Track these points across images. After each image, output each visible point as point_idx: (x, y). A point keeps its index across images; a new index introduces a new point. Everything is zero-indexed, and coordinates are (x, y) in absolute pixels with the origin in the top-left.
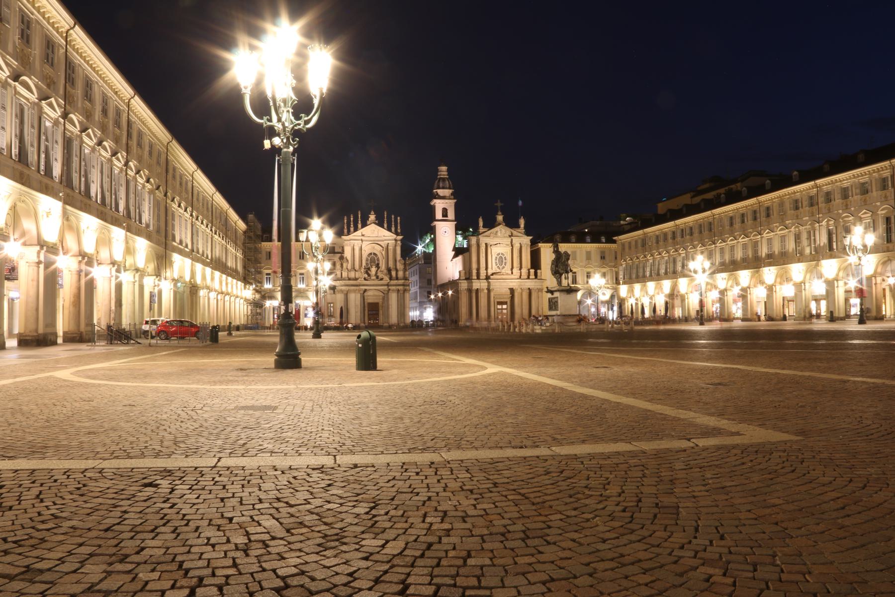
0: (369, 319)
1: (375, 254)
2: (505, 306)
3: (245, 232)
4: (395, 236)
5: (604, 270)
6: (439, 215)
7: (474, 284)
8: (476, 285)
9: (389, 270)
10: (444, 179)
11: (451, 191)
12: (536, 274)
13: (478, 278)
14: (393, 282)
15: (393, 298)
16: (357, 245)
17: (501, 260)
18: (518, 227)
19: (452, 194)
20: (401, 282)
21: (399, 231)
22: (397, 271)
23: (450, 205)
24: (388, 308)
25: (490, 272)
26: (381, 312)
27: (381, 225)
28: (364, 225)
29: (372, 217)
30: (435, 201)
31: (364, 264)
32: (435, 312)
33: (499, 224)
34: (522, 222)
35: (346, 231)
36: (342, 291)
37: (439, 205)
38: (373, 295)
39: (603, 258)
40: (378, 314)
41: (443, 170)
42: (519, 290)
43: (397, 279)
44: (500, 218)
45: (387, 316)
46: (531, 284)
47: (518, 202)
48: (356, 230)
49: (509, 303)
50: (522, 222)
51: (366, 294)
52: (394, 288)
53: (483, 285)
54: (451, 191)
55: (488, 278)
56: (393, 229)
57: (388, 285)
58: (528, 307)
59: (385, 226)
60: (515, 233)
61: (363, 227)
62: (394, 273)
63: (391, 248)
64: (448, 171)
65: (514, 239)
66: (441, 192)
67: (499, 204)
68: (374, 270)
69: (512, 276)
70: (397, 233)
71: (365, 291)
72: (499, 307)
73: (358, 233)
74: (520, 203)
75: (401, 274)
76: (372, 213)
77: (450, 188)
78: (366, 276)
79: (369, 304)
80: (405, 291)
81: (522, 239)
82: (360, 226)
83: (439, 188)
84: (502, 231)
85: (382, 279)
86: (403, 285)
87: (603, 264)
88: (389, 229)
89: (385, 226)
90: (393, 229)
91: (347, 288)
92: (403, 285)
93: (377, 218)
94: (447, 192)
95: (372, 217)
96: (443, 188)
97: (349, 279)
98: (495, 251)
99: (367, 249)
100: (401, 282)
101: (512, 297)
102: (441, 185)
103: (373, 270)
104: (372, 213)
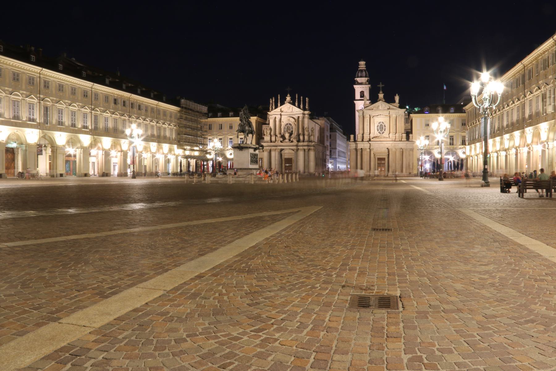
0: (286, 170)
1: (290, 124)
2: (383, 162)
3: (180, 112)
4: (302, 111)
5: (463, 134)
6: (358, 96)
7: (359, 145)
8: (360, 145)
9: (299, 135)
10: (362, 71)
11: (367, 79)
12: (408, 138)
13: (363, 141)
14: (300, 144)
15: (301, 154)
16: (278, 117)
17: (381, 128)
18: (394, 102)
19: (367, 81)
20: (306, 143)
21: (307, 107)
22: (304, 135)
23: (366, 89)
24: (297, 162)
25: (372, 136)
26: (294, 165)
27: (294, 104)
28: (282, 103)
29: (288, 98)
30: (355, 86)
31: (282, 131)
32: (431, 165)
33: (380, 100)
34: (397, 98)
35: (271, 109)
36: (266, 150)
37: (358, 89)
38: (288, 153)
39: (464, 124)
40: (291, 166)
41: (362, 64)
42: (394, 150)
43: (303, 141)
44: (381, 96)
45: (297, 167)
46: (403, 145)
47: (443, 87)
48: (276, 107)
49: (386, 160)
50: (397, 98)
51: (283, 152)
52: (301, 148)
53: (365, 145)
54: (367, 79)
55: (370, 140)
56: (301, 106)
57: (297, 146)
58: (400, 162)
59: (297, 104)
60: (391, 106)
61: (281, 105)
62: (301, 138)
63: (300, 119)
64: (366, 64)
65: (391, 111)
66: (359, 80)
67: (381, 86)
68: (287, 135)
69: (388, 139)
70: (304, 109)
71: (282, 150)
72: (379, 162)
73: (278, 109)
74: (445, 88)
75: (306, 138)
76: (288, 95)
77: (366, 77)
78: (282, 139)
79: (286, 159)
80: (309, 150)
81: (397, 111)
82: (279, 105)
83: (358, 77)
84: (381, 105)
85: (292, 142)
86: (308, 146)
87: (464, 129)
88: (299, 107)
89: (297, 104)
90: (301, 106)
91: (270, 148)
92: (308, 146)
93: (292, 99)
94: (364, 80)
95: (288, 98)
96: (361, 77)
97: (271, 142)
98: (377, 121)
99: (285, 120)
100: (306, 143)
101: (389, 155)
102: (359, 75)
103: (287, 135)
104: (288, 95)
